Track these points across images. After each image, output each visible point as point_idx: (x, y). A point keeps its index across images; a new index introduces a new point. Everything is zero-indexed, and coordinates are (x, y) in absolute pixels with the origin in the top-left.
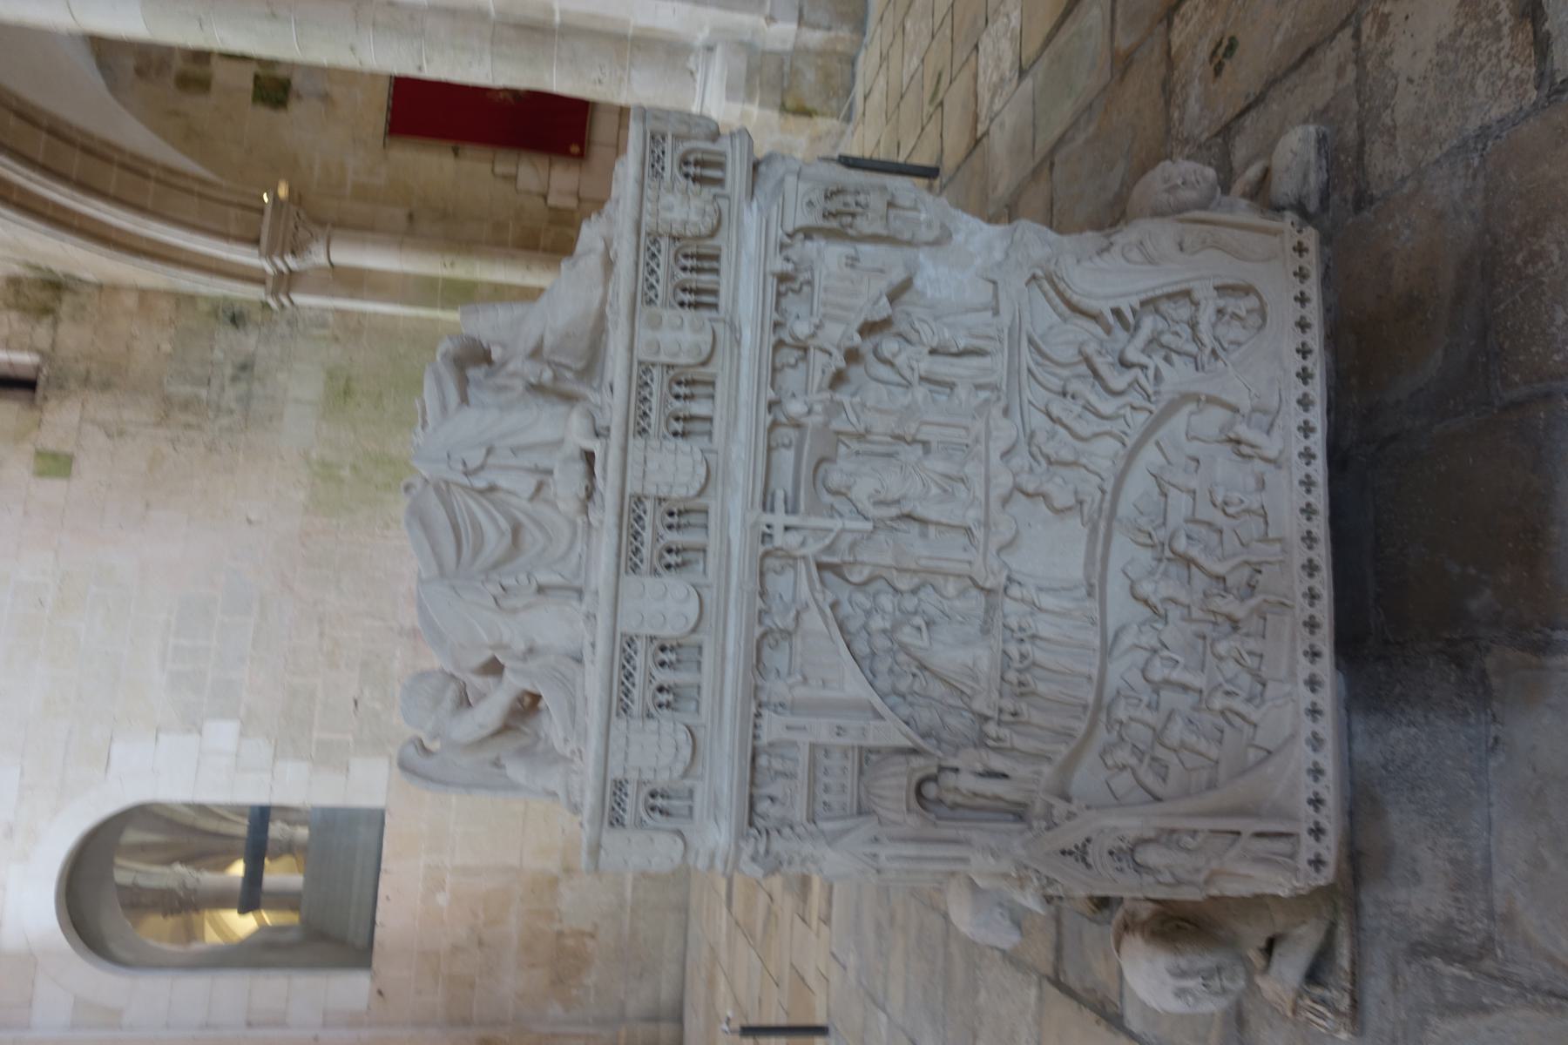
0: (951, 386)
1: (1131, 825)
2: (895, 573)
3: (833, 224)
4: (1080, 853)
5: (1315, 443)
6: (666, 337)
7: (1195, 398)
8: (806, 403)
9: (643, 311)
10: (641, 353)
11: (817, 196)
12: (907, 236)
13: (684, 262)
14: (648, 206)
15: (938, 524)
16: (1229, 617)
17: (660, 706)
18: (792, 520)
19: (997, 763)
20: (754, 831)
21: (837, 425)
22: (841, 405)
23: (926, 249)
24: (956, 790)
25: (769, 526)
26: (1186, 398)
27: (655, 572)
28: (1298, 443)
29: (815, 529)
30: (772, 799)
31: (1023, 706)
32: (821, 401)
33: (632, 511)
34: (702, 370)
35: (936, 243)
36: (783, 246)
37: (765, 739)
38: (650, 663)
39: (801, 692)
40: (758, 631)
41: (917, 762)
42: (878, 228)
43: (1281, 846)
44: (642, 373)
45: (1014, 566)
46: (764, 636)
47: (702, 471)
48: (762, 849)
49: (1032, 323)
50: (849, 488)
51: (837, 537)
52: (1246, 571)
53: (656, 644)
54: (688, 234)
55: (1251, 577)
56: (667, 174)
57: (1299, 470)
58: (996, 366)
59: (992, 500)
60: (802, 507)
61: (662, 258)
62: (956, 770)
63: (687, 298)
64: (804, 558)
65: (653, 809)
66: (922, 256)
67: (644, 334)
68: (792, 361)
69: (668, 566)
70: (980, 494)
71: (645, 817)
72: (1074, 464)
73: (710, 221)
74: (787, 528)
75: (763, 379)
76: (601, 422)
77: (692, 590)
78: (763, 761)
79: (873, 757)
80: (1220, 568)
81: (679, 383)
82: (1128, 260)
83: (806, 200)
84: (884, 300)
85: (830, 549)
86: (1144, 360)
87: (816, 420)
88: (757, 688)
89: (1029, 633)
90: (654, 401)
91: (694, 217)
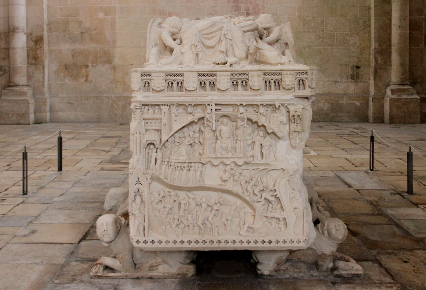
0: (253, 150)
1: (145, 195)
2: (203, 137)
3: (291, 117)
4: (139, 182)
5: (245, 244)
6: (256, 79)
7: (255, 212)
8: (243, 113)
9: (261, 73)
10: (251, 73)
11: (298, 113)
12: (291, 137)
13: (277, 82)
14: (288, 72)
15: (216, 146)
16: (197, 221)
17: (169, 83)
18: (214, 110)
19: (159, 162)
20: (141, 106)
21: (239, 120)
22: (244, 121)
23: (289, 143)
24: (152, 152)
25: (212, 105)
26: (254, 210)
27: (199, 80)
28: (245, 239)
29: (212, 116)
30: (148, 110)
31: (172, 167)
32: (244, 116)
33: (213, 74)
34: (249, 88)
35: (292, 145)
36: (283, 105)
37: (162, 107)
38: (178, 80)
39: (173, 115)
40: (187, 104)
41: (158, 142)
42: (292, 129)
43: (142, 233)
44: (246, 74)
45: (207, 166)
46: (186, 106)
47: (224, 89)
48: (137, 107)
49: (271, 170)
50: (223, 124)
51: (211, 122)
52: (210, 227)
53: (182, 81)
54: (282, 82)
55: (209, 228)
56: (298, 76)
57: (238, 239)
58: (258, 160)
59: (223, 159)
60: (217, 113)
61: (276, 76)
62: (157, 152)
63: (268, 83)
64: (205, 114)
65: (145, 83)
66: (288, 142)
67: (255, 74)
68: (255, 110)
69: (201, 83)
70: (224, 156)
71: (143, 82)
72: (234, 180)
73: (287, 87)
74: (212, 109)
75: (248, 102)
76: (233, 65)
77: (195, 88)
78: (157, 107)
79: (159, 133)
80: (210, 219)
81: (246, 82)
82: (290, 194)
83: (297, 111)
84: (272, 131)
85: (208, 121)
86: (263, 198)
87: (239, 115)
88: (174, 105)
89: (190, 168)
90: (240, 77)
91: (287, 83)
